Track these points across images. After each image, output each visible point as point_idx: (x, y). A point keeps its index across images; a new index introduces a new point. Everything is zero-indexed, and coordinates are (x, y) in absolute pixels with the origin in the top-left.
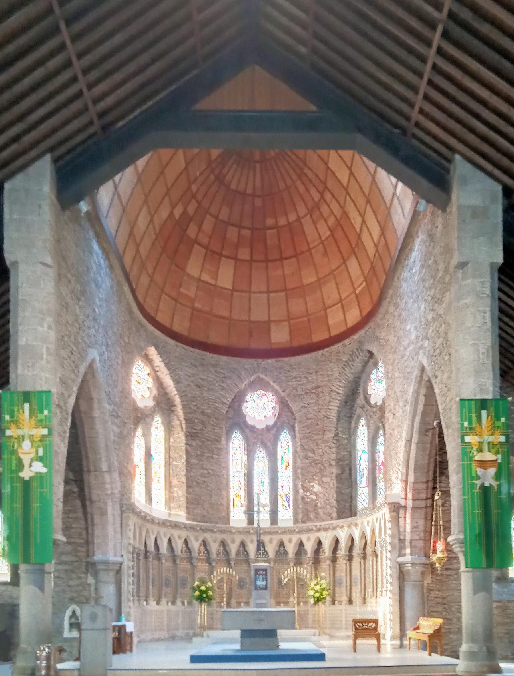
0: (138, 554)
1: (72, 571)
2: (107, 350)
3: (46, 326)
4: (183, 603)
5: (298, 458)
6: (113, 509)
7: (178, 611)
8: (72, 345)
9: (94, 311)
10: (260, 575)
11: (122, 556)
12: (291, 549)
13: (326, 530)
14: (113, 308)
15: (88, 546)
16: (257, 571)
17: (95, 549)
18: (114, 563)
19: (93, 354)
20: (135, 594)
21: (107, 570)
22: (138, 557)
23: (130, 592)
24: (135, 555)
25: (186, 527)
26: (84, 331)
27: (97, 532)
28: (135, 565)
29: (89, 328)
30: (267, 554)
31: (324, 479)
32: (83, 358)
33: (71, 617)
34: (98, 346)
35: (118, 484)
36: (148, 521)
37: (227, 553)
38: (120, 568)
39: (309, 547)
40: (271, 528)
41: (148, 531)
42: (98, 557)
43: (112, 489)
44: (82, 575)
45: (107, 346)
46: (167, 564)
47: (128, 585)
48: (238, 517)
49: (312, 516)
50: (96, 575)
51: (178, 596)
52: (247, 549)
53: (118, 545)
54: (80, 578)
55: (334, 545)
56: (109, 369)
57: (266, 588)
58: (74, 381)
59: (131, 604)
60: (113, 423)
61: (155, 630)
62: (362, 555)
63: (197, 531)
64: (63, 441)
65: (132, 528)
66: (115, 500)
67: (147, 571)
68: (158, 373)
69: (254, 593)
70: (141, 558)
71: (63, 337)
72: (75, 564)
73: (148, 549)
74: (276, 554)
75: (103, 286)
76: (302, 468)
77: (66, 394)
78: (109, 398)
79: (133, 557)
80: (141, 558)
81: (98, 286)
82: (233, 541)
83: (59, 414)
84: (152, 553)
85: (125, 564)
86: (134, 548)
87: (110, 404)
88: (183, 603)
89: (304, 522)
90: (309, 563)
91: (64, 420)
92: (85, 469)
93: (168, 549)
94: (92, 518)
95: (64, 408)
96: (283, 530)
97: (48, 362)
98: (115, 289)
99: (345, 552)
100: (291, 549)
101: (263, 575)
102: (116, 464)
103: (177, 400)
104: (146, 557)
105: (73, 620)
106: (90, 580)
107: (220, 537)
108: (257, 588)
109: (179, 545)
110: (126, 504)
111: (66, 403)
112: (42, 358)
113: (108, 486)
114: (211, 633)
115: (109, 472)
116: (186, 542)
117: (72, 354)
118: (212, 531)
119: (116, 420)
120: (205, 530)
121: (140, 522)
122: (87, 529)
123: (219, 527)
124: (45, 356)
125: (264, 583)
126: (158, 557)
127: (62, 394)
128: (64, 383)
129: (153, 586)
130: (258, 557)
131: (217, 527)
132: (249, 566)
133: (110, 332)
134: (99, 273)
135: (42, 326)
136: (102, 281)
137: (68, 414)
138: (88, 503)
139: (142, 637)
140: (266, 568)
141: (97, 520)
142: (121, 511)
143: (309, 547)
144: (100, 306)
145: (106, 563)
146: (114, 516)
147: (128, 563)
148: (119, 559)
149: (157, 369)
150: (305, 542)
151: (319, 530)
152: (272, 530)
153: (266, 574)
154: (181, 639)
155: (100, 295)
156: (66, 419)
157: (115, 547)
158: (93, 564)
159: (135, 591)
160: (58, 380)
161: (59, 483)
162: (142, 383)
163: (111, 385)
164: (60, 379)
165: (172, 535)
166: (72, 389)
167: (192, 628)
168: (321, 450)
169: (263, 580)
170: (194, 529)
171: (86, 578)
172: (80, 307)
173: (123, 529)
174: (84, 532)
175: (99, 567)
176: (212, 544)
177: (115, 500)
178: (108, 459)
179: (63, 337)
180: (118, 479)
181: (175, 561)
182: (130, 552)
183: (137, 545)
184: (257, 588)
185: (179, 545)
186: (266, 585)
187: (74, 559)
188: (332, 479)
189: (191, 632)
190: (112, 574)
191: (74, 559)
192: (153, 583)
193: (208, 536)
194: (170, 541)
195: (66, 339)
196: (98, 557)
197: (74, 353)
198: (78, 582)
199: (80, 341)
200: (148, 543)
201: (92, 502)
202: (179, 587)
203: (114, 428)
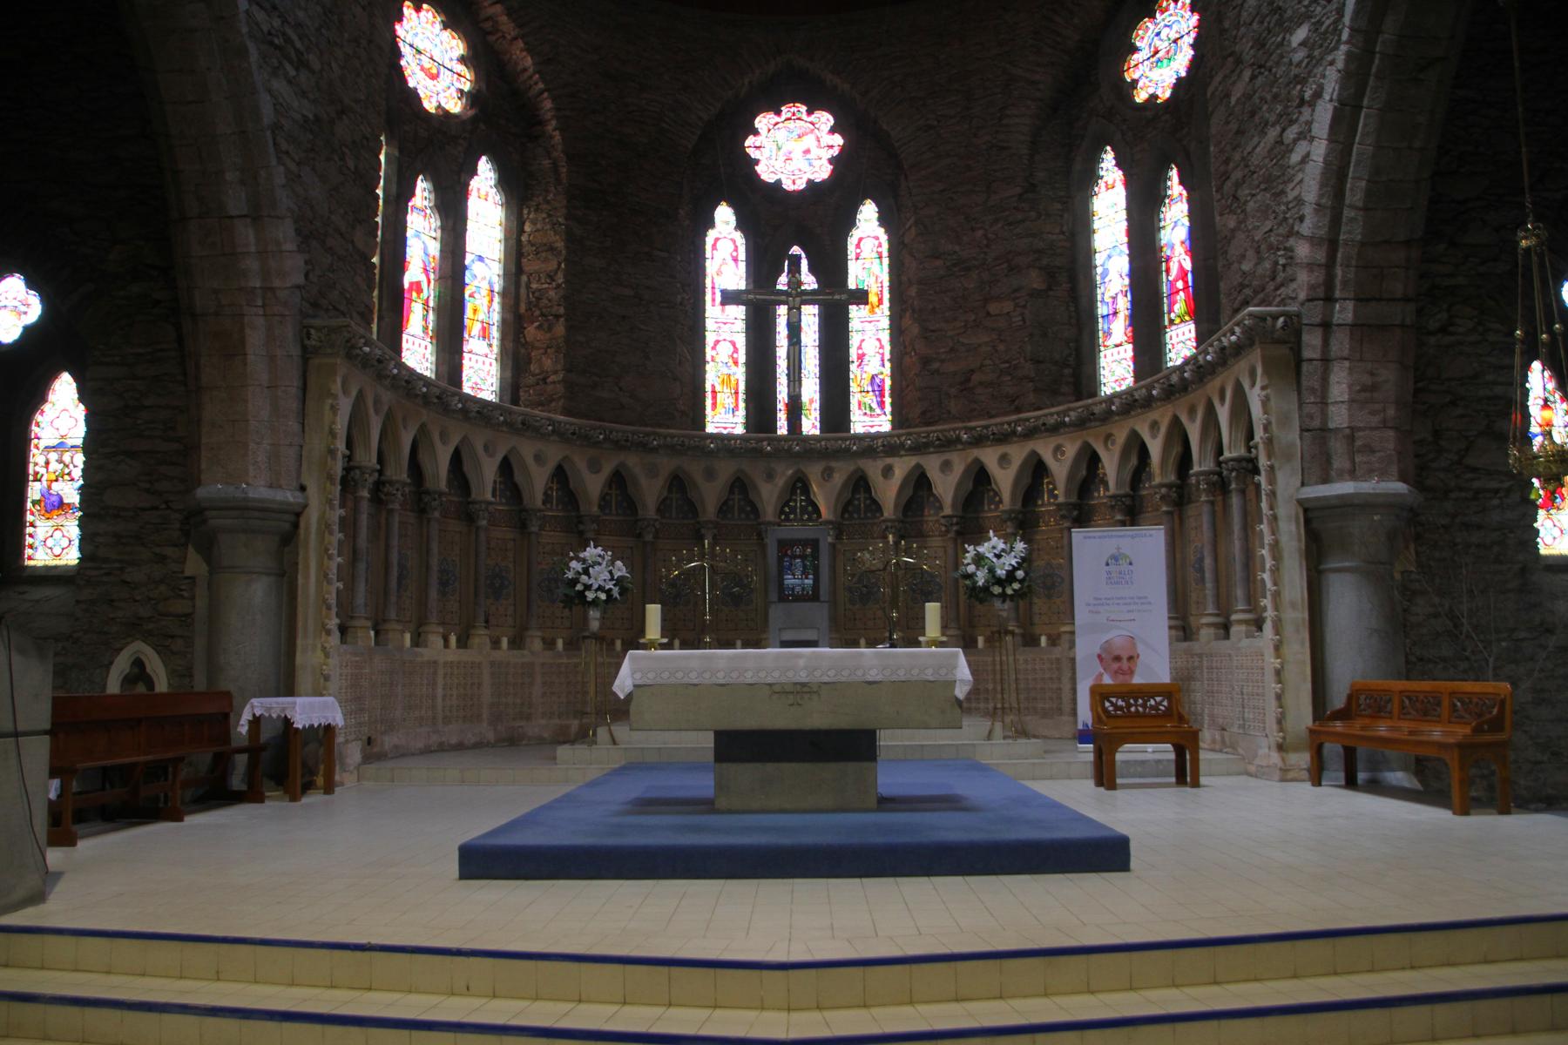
10: (796, 557)
12: (888, 492)
18: (265, 509)
25: (559, 434)
30: (817, 510)
31: (993, 308)
37: (691, 508)
39: (946, 486)
42: (212, 489)
48: (725, 416)
50: (208, 549)
52: (752, 496)
54: (162, 559)
55: (1027, 481)
57: (814, 596)
61: (447, 720)
62: (1128, 502)
63: (597, 444)
68: (492, 38)
69: (777, 612)
74: (845, 510)
82: (710, 474)
85: (312, 517)
88: (549, 644)
90: (947, 531)
100: (888, 492)
101: (803, 557)
106: (194, 564)
107: (667, 464)
108: (785, 596)
113: (252, 264)
115: (256, 216)
116: (560, 474)
118: (644, 447)
120: (619, 446)
125: (809, 582)
131: (659, 435)
143: (946, 486)
145: (243, 508)
147: (321, 509)
148: (290, 496)
149: (488, 26)
150: (934, 474)
151: (979, 441)
153: (815, 555)
168: (981, 232)
169: (805, 574)
176: (644, 481)
181: (523, 526)
184: (785, 596)
188: (1017, 305)
193: (633, 461)
196: (212, 489)
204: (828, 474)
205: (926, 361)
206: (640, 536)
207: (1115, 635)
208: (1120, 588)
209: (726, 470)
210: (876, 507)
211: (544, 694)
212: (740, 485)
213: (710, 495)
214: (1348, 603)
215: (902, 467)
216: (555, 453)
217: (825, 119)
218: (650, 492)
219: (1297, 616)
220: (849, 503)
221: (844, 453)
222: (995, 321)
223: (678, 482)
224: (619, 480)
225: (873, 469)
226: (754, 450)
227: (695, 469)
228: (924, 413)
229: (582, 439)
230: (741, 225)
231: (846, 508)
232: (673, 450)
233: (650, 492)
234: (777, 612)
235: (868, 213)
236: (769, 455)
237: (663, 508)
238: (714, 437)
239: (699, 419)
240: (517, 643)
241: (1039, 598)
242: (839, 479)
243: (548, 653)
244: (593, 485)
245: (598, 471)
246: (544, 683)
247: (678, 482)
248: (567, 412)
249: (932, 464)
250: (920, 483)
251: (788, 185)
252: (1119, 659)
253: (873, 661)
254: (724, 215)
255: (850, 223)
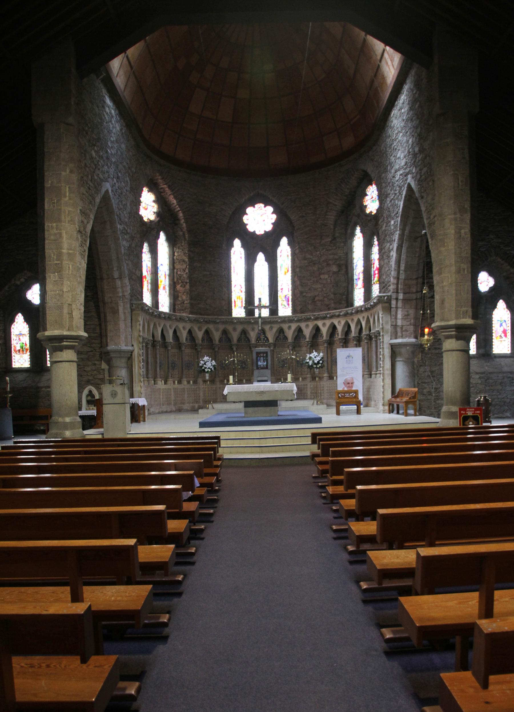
0: (147, 344)
1: (88, 359)
2: (117, 182)
3: (68, 171)
4: (189, 382)
5: (296, 259)
6: (124, 308)
7: (184, 389)
8: (89, 182)
9: (107, 152)
11: (133, 346)
12: (290, 334)
13: (324, 318)
14: (123, 146)
15: (101, 338)
16: (258, 353)
17: (109, 341)
19: (107, 186)
20: (145, 376)
21: (120, 357)
22: (146, 346)
23: (140, 374)
24: (144, 345)
26: (99, 169)
27: (110, 327)
28: (145, 352)
29: (103, 166)
30: (268, 339)
32: (97, 189)
33: (87, 396)
34: (110, 180)
35: (129, 288)
36: (155, 316)
37: (229, 340)
38: (131, 355)
39: (307, 332)
40: (271, 318)
41: (155, 325)
43: (123, 292)
44: (96, 362)
45: (118, 178)
46: (173, 351)
47: (138, 369)
48: (238, 311)
49: (310, 307)
51: (184, 376)
52: (248, 336)
53: (129, 337)
55: (331, 331)
56: (119, 196)
57: (267, 368)
58: (91, 210)
59: (142, 384)
60: (124, 239)
64: (83, 258)
65: (141, 322)
66: (126, 300)
67: (155, 358)
70: (149, 346)
71: (82, 177)
72: (91, 353)
73: (156, 339)
74: (276, 339)
75: (114, 131)
76: (300, 267)
77: (85, 222)
78: (120, 219)
79: (143, 346)
80: (149, 346)
81: (110, 132)
83: (79, 237)
84: (159, 341)
86: (143, 339)
87: (120, 224)
88: (189, 382)
89: (303, 312)
90: (307, 346)
91: (84, 242)
92: (99, 277)
93: (173, 338)
94: (105, 316)
95: (83, 232)
96: (282, 319)
97: (70, 199)
98: (123, 131)
99: (342, 335)
100: (290, 334)
101: (263, 357)
102: (126, 272)
103: (181, 215)
104: (154, 346)
105: (89, 398)
108: (258, 368)
109: (184, 335)
110: (135, 304)
111: (85, 228)
112: (65, 196)
114: (215, 406)
116: (190, 332)
117: (89, 189)
118: (215, 322)
119: (125, 237)
120: (207, 322)
121: (148, 317)
122: (100, 325)
123: (221, 319)
124: (67, 194)
125: (265, 363)
126: (165, 345)
127: (82, 222)
128: (84, 213)
129: (160, 369)
130: (259, 342)
131: (219, 319)
132: (252, 352)
133: (120, 166)
134: (111, 121)
135: (65, 171)
136: (113, 127)
137: (86, 237)
138: (101, 304)
139: (152, 410)
140: (266, 351)
141: (109, 318)
142: (131, 309)
144: (112, 147)
146: (125, 313)
151: (316, 319)
152: (272, 320)
154: (187, 411)
155: (112, 139)
156: (86, 241)
157: (126, 338)
158: (108, 353)
159: (145, 373)
160: (79, 211)
161: (81, 291)
162: (148, 207)
163: (121, 209)
164: (80, 210)
165: (177, 326)
166: (89, 217)
167: (197, 402)
169: (264, 361)
170: (198, 321)
171: (101, 365)
172: (95, 151)
173: (133, 324)
174: (98, 328)
175: (112, 355)
177: (126, 300)
178: (119, 268)
179: (82, 177)
180: (128, 284)
182: (140, 342)
183: (146, 336)
185: (184, 335)
186: (267, 365)
187: (90, 349)
189: (196, 405)
190: (124, 360)
191: (90, 349)
192: (160, 366)
193: (211, 327)
194: (175, 332)
195: (85, 178)
197: (91, 188)
198: (94, 368)
199: (96, 178)
200: (155, 334)
201: (104, 303)
202: (184, 368)
203: (124, 243)
204: (271, 328)
205: (301, 293)
206: (214, 349)
207: (348, 377)
208: (349, 363)
209: (240, 328)
210: (286, 338)
211: (188, 397)
212: (244, 332)
213: (235, 336)
214: (401, 369)
215: (294, 326)
216: (188, 326)
217: (270, 209)
218: (217, 336)
219: (388, 372)
220: (278, 337)
221: (276, 322)
222: (322, 281)
223: (225, 332)
224: (207, 332)
225: (285, 326)
226: (248, 322)
227: (230, 328)
228: (301, 309)
229: (196, 321)
230: (243, 246)
231: (277, 339)
232: (224, 323)
233: (217, 336)
234: (256, 372)
235: (284, 241)
236: (253, 323)
237: (220, 340)
238: (236, 318)
239: (230, 313)
240: (180, 382)
241: (329, 366)
242: (275, 330)
243: (189, 385)
244: (200, 335)
245: (201, 331)
246: (188, 394)
247: (225, 332)
248: (191, 313)
249: (303, 325)
250: (300, 330)
251: (258, 233)
252: (349, 383)
253: (278, 386)
254: (237, 243)
255: (278, 245)
